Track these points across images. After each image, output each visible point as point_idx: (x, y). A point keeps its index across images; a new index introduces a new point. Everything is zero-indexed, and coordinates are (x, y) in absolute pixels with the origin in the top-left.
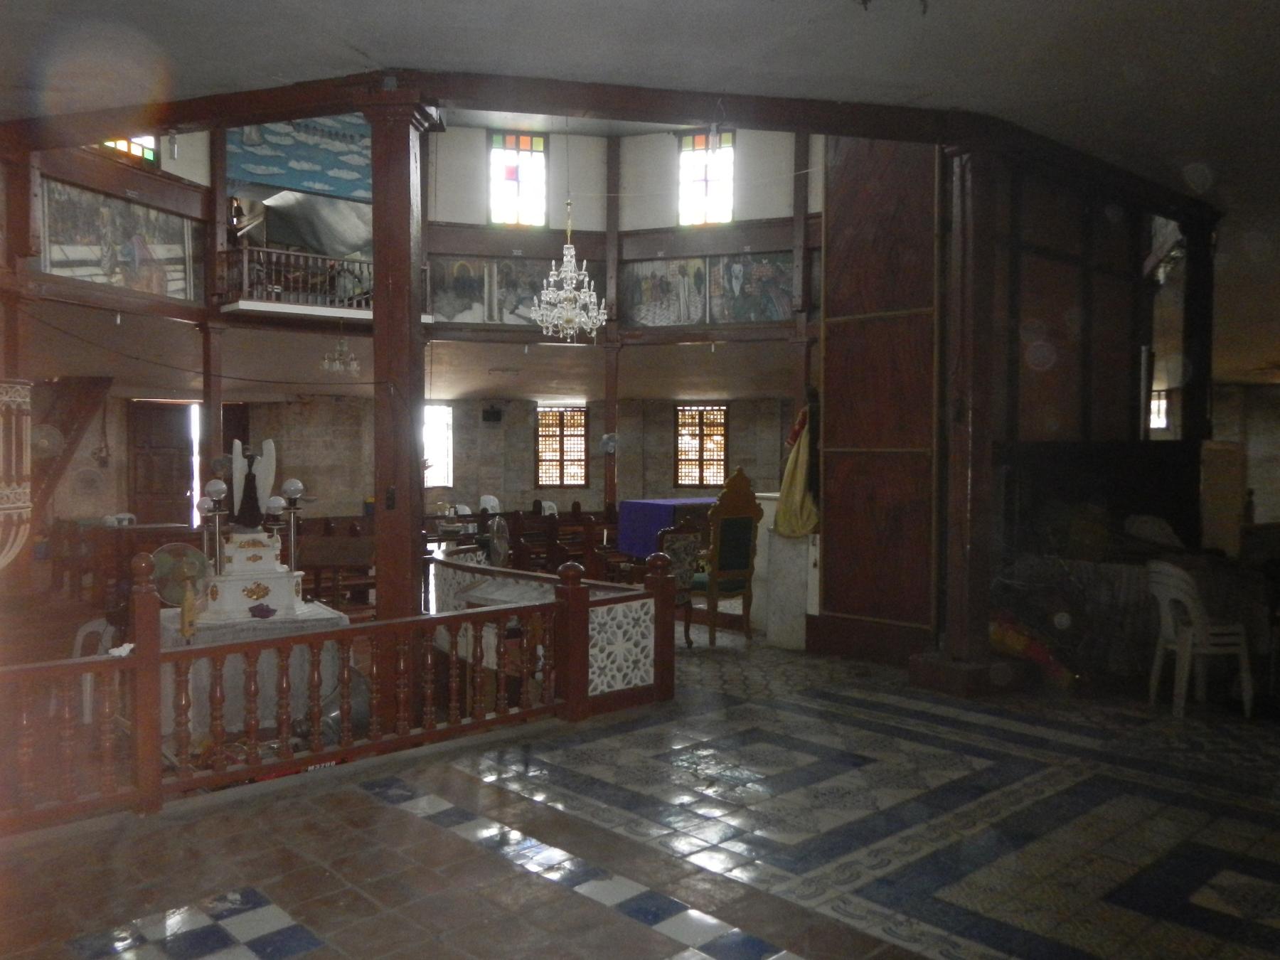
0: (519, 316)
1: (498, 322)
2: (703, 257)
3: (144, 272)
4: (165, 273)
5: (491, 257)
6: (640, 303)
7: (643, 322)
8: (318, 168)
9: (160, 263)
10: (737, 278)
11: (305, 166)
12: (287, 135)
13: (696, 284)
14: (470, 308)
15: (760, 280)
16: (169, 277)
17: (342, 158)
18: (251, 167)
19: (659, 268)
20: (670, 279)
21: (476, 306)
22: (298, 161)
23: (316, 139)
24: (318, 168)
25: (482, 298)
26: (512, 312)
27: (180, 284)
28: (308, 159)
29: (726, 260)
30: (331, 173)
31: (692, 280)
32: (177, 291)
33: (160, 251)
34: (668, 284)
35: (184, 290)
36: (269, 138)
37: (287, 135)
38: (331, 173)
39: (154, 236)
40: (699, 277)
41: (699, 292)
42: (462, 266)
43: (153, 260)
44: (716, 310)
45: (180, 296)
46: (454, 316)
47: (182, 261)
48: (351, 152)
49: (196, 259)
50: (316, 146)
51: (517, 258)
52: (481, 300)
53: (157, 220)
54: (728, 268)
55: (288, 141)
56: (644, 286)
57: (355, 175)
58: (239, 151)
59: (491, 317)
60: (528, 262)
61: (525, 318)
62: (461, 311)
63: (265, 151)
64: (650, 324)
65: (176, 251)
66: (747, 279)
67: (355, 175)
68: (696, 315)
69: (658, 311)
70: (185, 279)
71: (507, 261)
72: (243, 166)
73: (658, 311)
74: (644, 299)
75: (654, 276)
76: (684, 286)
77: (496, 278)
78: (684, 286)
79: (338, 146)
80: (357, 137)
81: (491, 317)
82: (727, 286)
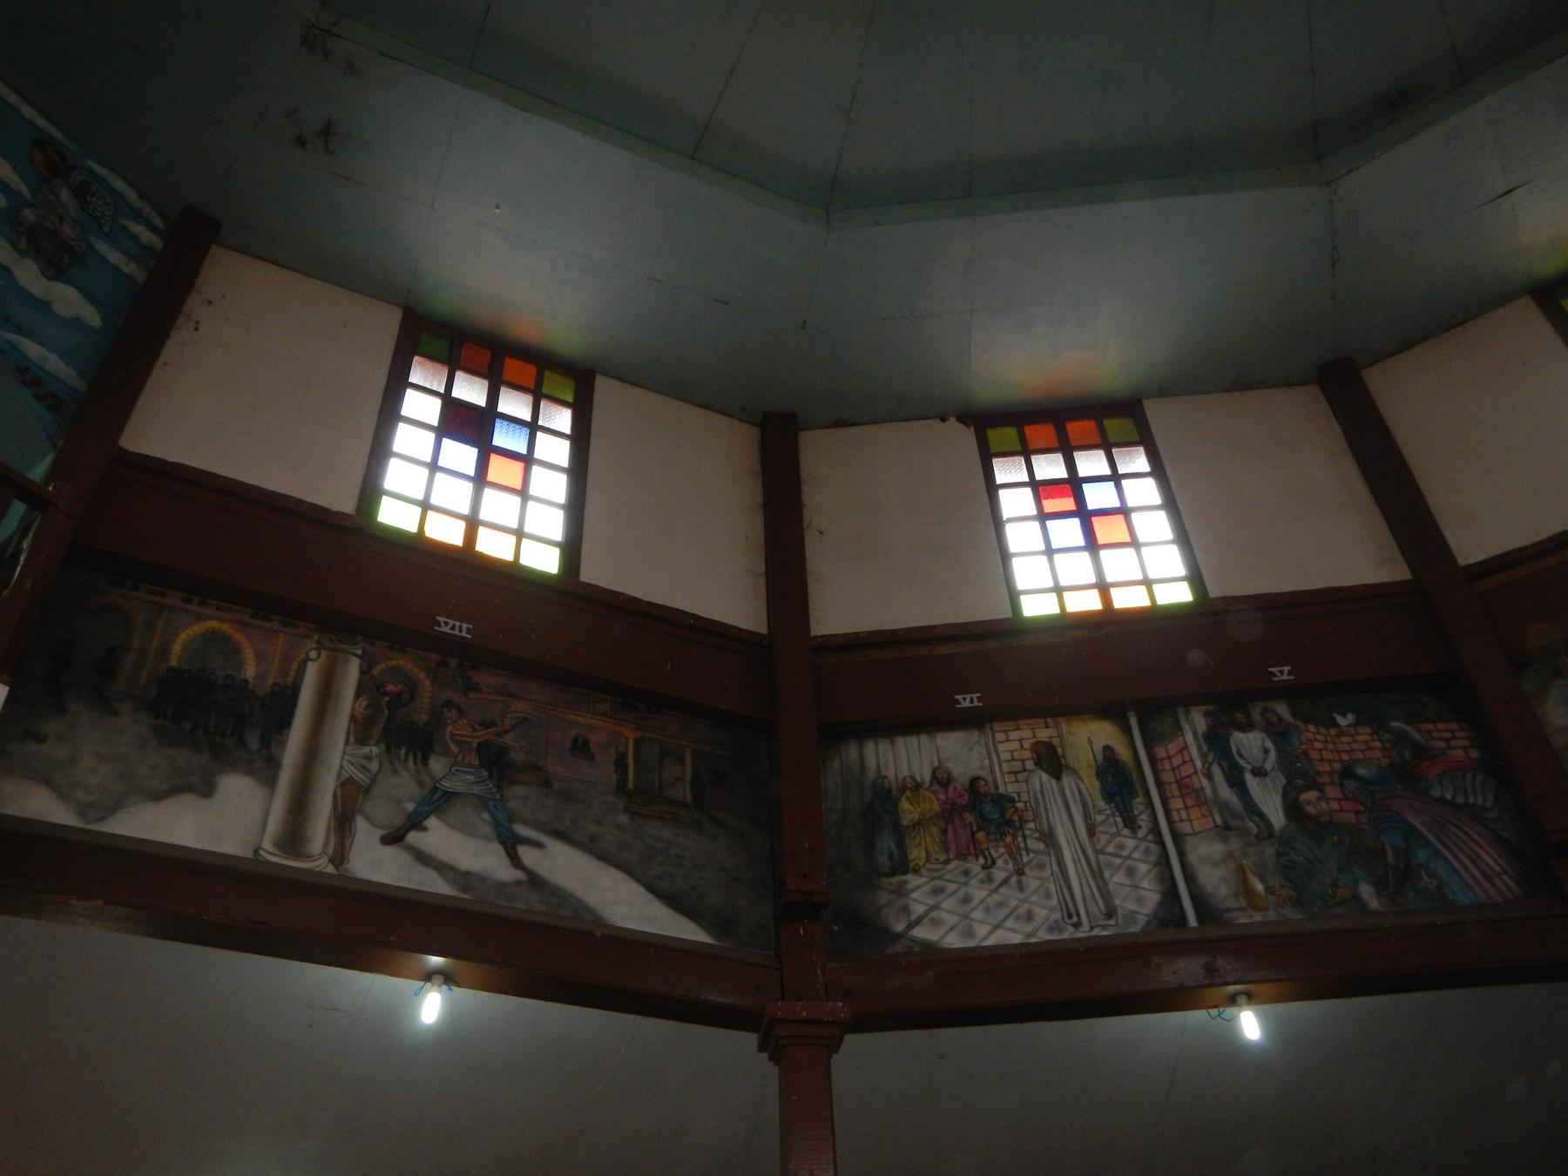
0: (423, 858)
1: (323, 865)
2: (1113, 712)
5: (339, 626)
6: (902, 866)
7: (920, 933)
10: (1259, 772)
13: (1108, 796)
14: (206, 789)
15: (1348, 773)
19: (959, 753)
20: (1008, 787)
25: (274, 764)
26: (394, 838)
29: (1197, 721)
31: (1092, 786)
34: (1004, 801)
40: (1118, 782)
41: (1131, 823)
42: (213, 635)
44: (1216, 880)
46: (116, 806)
51: (448, 646)
52: (267, 772)
54: (1216, 741)
56: (909, 811)
59: (293, 839)
60: (486, 679)
61: (444, 869)
62: (157, 796)
64: (954, 941)
66: (1298, 775)
68: (1138, 899)
69: (978, 893)
73: (978, 893)
74: (916, 854)
75: (941, 779)
76: (1066, 808)
78: (1066, 808)
81: (293, 839)
82: (1226, 793)
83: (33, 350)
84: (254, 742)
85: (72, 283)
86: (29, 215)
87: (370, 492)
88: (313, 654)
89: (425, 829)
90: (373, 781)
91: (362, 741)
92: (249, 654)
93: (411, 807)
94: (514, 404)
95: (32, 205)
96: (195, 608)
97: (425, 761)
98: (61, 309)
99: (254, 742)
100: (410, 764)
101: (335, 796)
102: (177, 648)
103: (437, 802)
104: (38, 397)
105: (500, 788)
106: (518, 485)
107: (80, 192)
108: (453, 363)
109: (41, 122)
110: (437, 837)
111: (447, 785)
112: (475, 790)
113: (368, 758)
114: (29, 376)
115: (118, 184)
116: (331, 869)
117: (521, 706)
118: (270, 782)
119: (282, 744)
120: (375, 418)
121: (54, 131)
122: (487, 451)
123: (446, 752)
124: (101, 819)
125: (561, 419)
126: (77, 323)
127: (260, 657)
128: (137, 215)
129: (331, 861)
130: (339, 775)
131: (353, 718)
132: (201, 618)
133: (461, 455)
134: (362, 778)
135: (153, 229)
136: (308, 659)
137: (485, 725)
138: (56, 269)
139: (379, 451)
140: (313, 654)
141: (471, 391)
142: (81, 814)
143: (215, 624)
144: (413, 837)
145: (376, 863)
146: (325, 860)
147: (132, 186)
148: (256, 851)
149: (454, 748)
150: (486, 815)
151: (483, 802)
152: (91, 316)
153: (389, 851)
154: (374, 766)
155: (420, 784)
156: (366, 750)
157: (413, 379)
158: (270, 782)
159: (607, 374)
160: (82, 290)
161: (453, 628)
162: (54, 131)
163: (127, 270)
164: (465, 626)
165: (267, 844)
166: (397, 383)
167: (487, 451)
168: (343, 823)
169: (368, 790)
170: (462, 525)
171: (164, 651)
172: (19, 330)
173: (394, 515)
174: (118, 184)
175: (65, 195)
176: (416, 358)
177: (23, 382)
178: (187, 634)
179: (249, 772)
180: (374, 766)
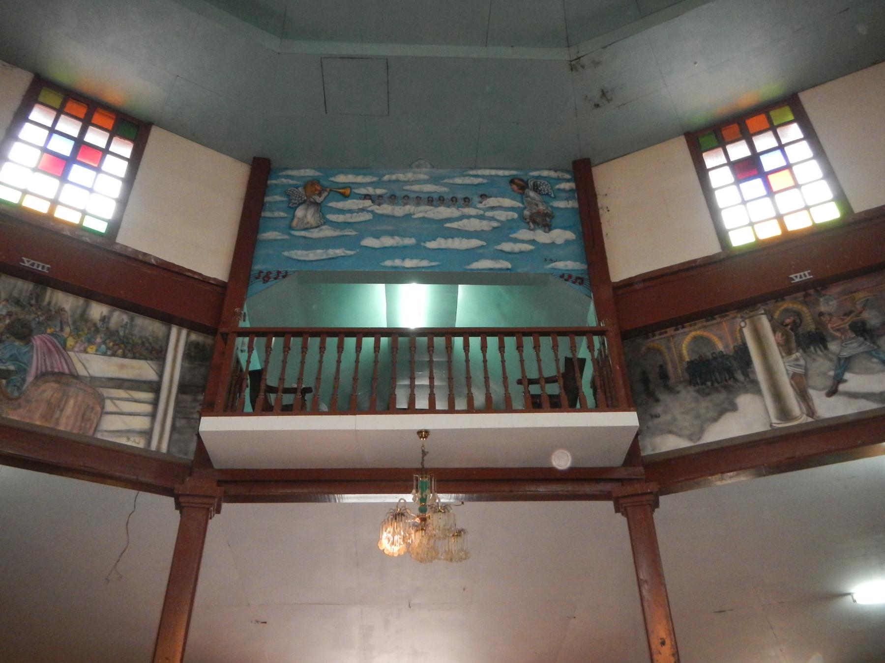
1: (805, 419)
3: (49, 391)
4: (101, 400)
5: (747, 305)
8: (410, 241)
9: (95, 383)
11: (388, 241)
12: (363, 210)
14: (734, 408)
16: (109, 406)
17: (448, 225)
18: (299, 254)
21: (745, 401)
22: (377, 237)
23: (409, 208)
24: (410, 241)
25: (755, 383)
26: (833, 392)
27: (142, 423)
28: (392, 234)
30: (431, 245)
32: (128, 432)
33: (97, 364)
35: (147, 434)
36: (332, 217)
37: (363, 210)
38: (431, 245)
39: (90, 342)
42: (696, 339)
43: (77, 377)
45: (138, 443)
46: (702, 431)
47: (155, 388)
48: (469, 217)
49: (183, 388)
50: (408, 216)
51: (803, 287)
52: (754, 387)
53: (104, 319)
55: (367, 217)
57: (475, 243)
58: (286, 237)
59: (784, 413)
62: (715, 420)
63: (327, 232)
65: (145, 370)
67: (475, 243)
70: (153, 416)
71: (787, 304)
72: (286, 254)
77: (772, 339)
79: (443, 212)
80: (476, 199)
81: (784, 413)
83: (561, 265)
84: (740, 376)
85: (556, 228)
86: (527, 213)
87: (722, 236)
88: (743, 324)
89: (845, 381)
90: (806, 369)
91: (789, 352)
92: (715, 339)
93: (832, 373)
94: (764, 141)
95: (525, 208)
96: (681, 331)
97: (826, 348)
98: (560, 241)
99: (740, 376)
100: (819, 352)
101: (792, 385)
102: (685, 352)
103: (844, 364)
104: (574, 282)
105: (874, 343)
106: (792, 183)
107: (536, 188)
108: (722, 143)
109: (507, 173)
110: (854, 382)
111: (845, 354)
112: (861, 349)
113: (797, 360)
114: (566, 277)
115: (545, 173)
116: (810, 420)
117: (861, 295)
118: (759, 392)
119: (754, 372)
120: (703, 197)
121: (514, 172)
122: (764, 176)
123: (834, 338)
124: (700, 438)
125: (793, 131)
126: (568, 242)
127: (721, 338)
128: (560, 180)
129: (808, 415)
130: (788, 374)
131: (779, 344)
132: (687, 334)
133: (755, 186)
134: (799, 370)
135: (568, 181)
136: (741, 328)
137: (847, 314)
138: (548, 228)
139: (714, 211)
140: (743, 324)
141: (739, 151)
142: (691, 440)
143: (693, 333)
144: (842, 387)
145: (830, 408)
146: (805, 416)
147: (550, 169)
148: (771, 426)
149: (838, 334)
150: (875, 360)
151: (869, 354)
152: (570, 235)
153: (833, 399)
154: (802, 362)
155: (831, 360)
156: (794, 356)
157: (708, 166)
158: (759, 392)
159: (803, 90)
160: (561, 228)
161: (801, 277)
162: (514, 172)
163: (569, 206)
164: (806, 273)
165: (774, 420)
166: (702, 172)
167: (764, 176)
168: (803, 395)
169: (806, 375)
170: (775, 222)
171: (681, 356)
172: (552, 261)
173: (739, 239)
174: (545, 173)
175: (532, 194)
176: (704, 154)
177: (566, 280)
178: (684, 344)
179: (746, 391)
180: (802, 362)
